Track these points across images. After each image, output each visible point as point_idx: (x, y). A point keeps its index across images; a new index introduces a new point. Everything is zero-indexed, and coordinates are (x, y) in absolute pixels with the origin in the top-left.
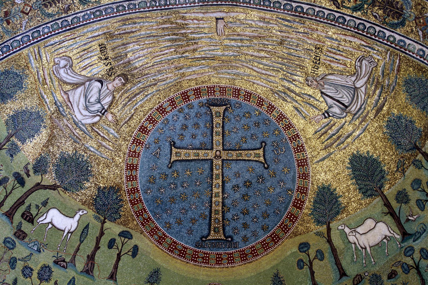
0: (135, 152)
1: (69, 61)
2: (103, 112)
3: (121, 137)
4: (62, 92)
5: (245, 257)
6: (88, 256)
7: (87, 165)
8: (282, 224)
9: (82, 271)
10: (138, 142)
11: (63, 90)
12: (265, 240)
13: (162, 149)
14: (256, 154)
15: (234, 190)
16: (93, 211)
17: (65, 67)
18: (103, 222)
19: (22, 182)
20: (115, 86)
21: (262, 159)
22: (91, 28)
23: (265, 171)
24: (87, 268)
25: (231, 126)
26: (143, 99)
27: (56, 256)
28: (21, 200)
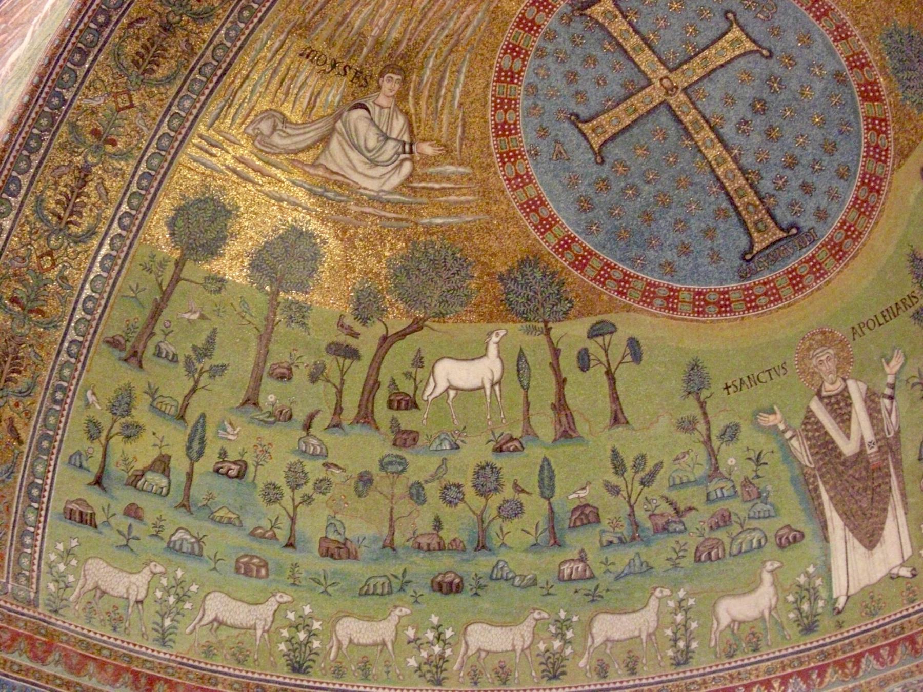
0: (518, 176)
1: (274, 116)
2: (408, 149)
3: (472, 167)
4: (307, 169)
5: (839, 251)
6: (554, 407)
7: (450, 252)
8: (868, 147)
9: (555, 440)
10: (511, 157)
11: (306, 165)
12: (857, 198)
13: (562, 140)
14: (732, 43)
15: (744, 131)
16: (514, 322)
17: (274, 129)
18: (548, 330)
19: (353, 354)
20: (391, 94)
21: (749, 45)
22: (259, 43)
23: (771, 62)
24: (563, 428)
25: (650, 21)
26: (458, 81)
27: (492, 438)
28: (371, 382)
